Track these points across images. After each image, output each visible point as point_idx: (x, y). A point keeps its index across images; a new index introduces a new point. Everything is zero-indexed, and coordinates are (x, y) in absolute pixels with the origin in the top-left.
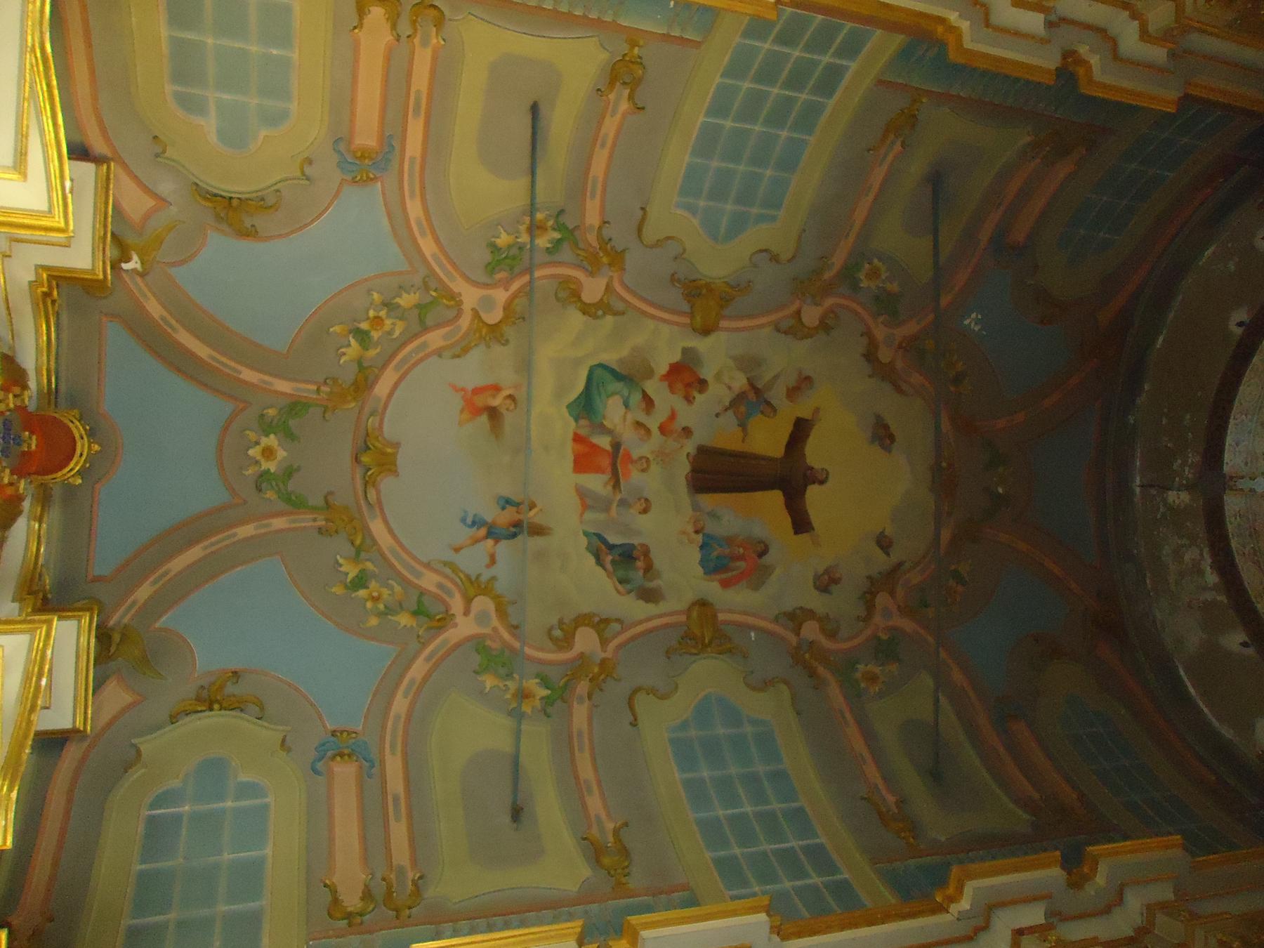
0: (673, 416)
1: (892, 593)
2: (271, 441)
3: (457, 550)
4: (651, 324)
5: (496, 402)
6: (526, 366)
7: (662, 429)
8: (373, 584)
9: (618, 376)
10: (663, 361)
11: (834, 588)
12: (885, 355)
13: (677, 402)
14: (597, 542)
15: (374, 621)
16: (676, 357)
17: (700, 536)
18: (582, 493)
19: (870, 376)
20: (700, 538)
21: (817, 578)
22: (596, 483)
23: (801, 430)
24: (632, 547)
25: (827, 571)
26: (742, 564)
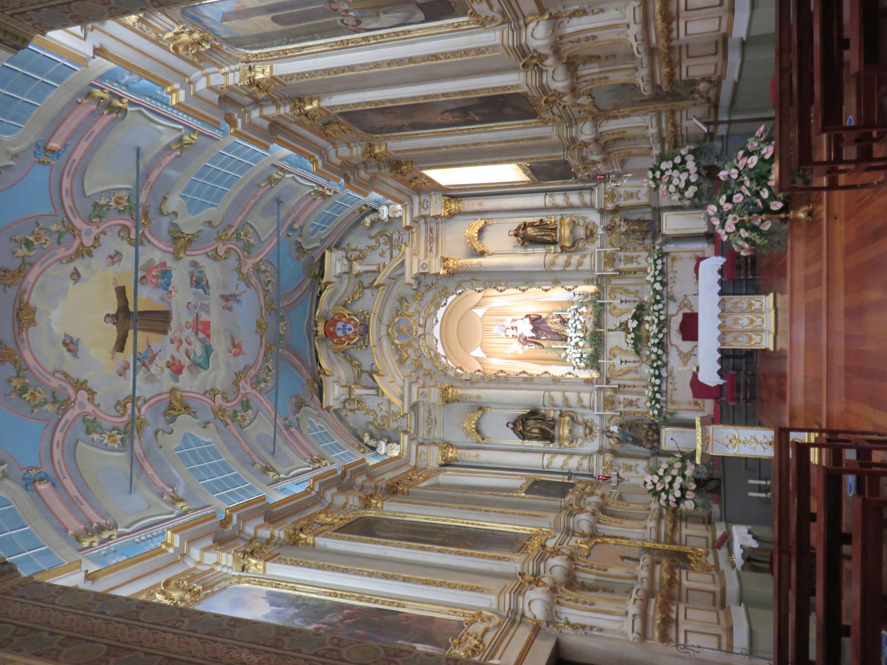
0: (178, 348)
1: (82, 243)
2: (282, 332)
3: (245, 291)
4: (193, 390)
5: (234, 350)
6: (228, 365)
7: (181, 342)
8: (266, 281)
9: (199, 365)
10: (185, 373)
11: (112, 253)
12: (83, 395)
13: (178, 357)
14: (207, 290)
15: (269, 269)
16: (181, 377)
17: (170, 289)
18: (208, 312)
19: (86, 381)
20: (170, 288)
21: (120, 260)
22: (204, 317)
23: (120, 346)
24: (195, 287)
25: (114, 263)
26: (154, 273)
